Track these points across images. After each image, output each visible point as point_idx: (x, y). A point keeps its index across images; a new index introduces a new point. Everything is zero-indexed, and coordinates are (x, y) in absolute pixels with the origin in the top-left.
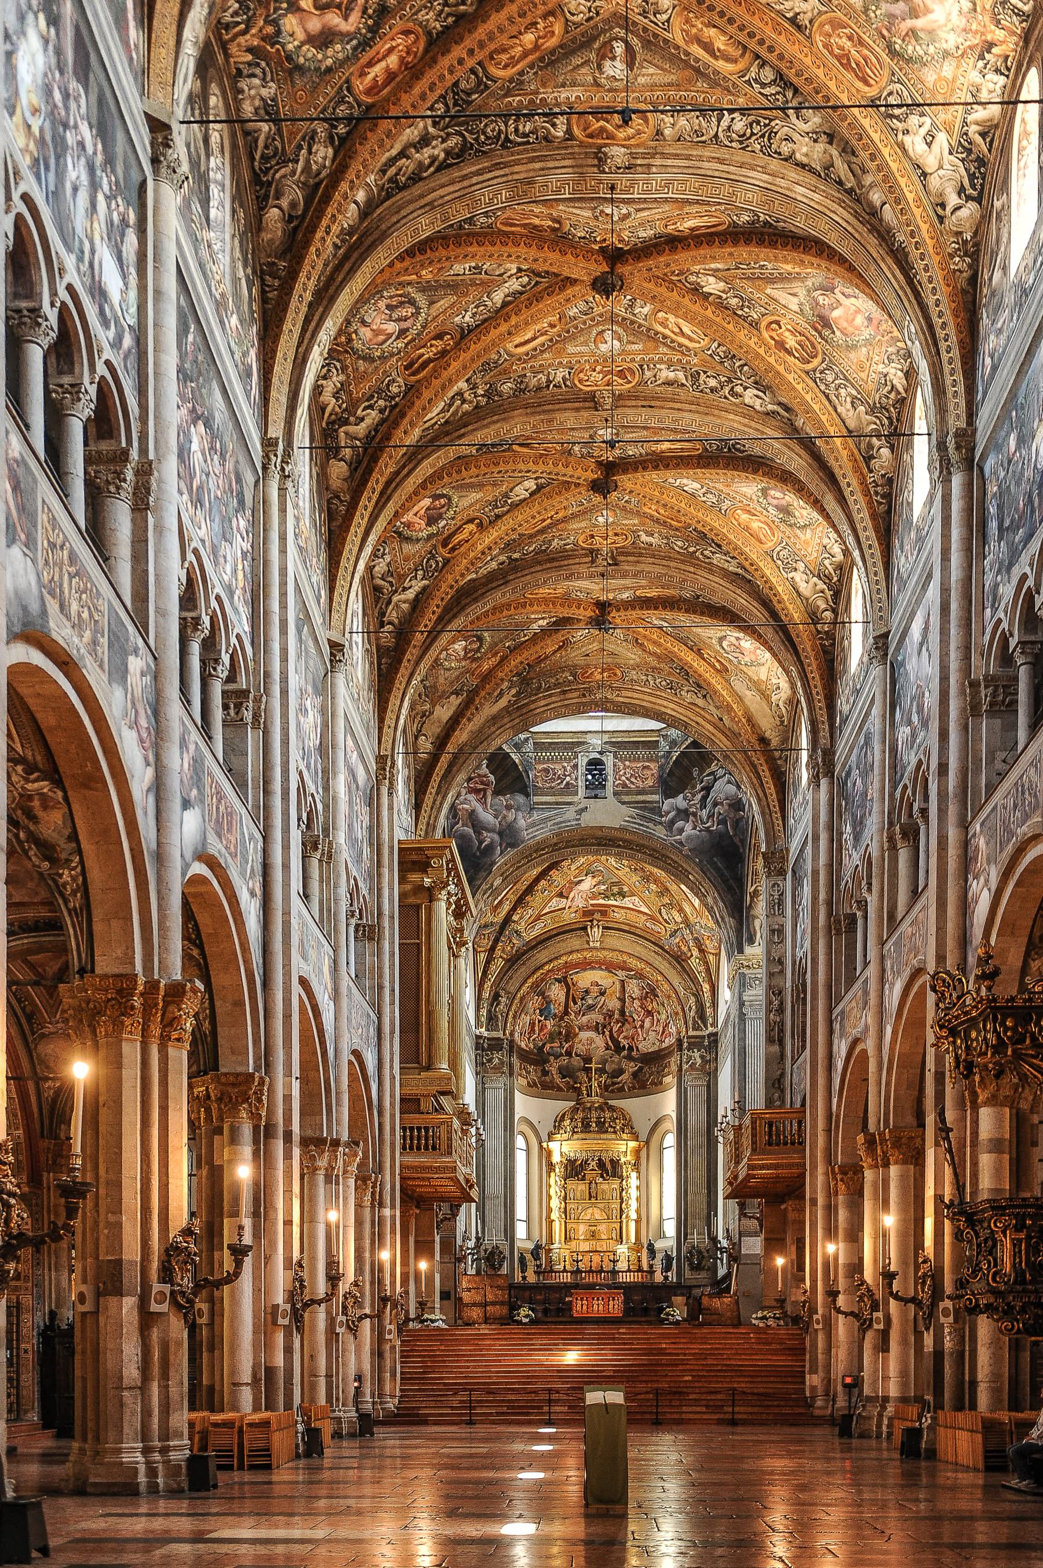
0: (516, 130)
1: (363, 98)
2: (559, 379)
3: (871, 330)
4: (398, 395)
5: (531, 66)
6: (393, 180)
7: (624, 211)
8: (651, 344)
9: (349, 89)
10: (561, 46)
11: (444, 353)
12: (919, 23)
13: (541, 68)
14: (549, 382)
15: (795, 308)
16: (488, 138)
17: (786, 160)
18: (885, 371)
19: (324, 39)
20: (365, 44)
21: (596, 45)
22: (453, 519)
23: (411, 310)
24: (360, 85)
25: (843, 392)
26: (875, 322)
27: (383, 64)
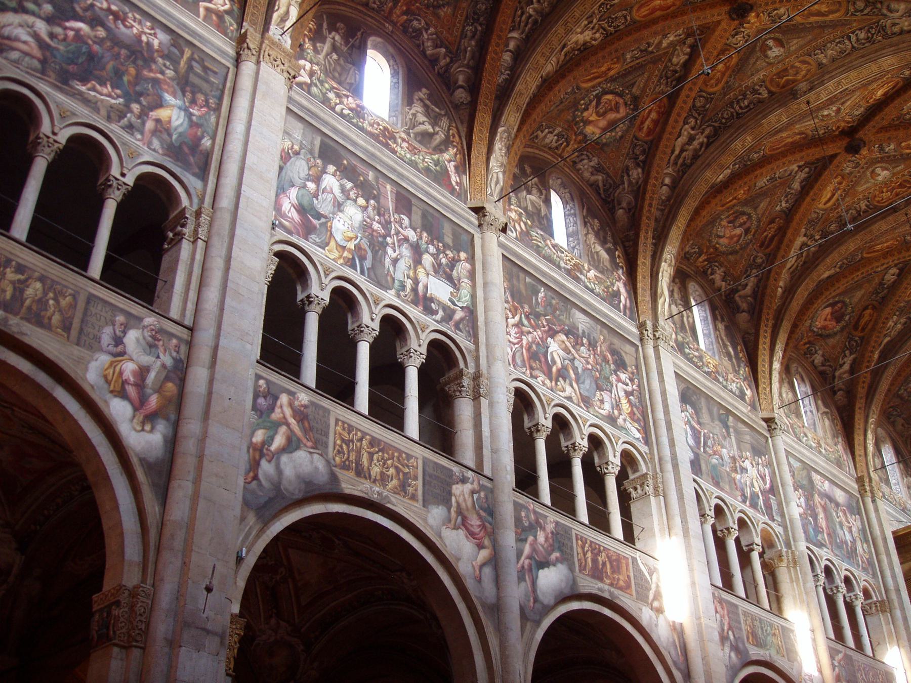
1: (647, 139)
9: (637, 139)
11: (780, 228)
16: (726, 119)
19: (612, 125)
22: (853, 312)
23: (745, 218)
24: (642, 135)
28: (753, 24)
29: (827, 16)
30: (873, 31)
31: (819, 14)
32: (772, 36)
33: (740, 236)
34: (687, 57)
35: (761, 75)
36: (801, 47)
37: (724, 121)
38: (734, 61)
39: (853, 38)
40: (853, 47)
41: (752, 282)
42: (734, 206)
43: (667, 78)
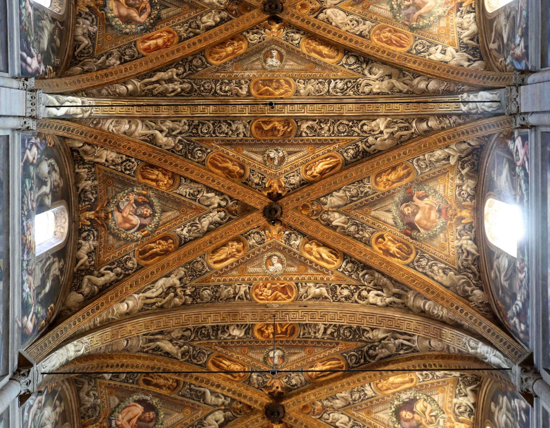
0: (221, 89)
2: (242, 292)
3: (443, 220)
4: (132, 269)
5: (230, 61)
6: (151, 91)
7: (281, 154)
8: (302, 267)
10: (246, 53)
12: (422, 11)
13: (235, 62)
14: (235, 294)
15: (391, 221)
16: (205, 89)
17: (368, 94)
18: (459, 244)
20: (147, 30)
21: (263, 52)
25: (435, 268)
26: (444, 211)
27: (155, 41)
28: (272, 32)
29: (324, 57)
30: (349, 85)
31: (320, 53)
32: (279, 49)
33: (133, 226)
34: (214, 24)
35: (251, 74)
36: (293, 70)
37: (202, 88)
38: (241, 51)
39: (332, 85)
40: (328, 91)
41: (110, 276)
42: (151, 188)
43: (190, 27)
